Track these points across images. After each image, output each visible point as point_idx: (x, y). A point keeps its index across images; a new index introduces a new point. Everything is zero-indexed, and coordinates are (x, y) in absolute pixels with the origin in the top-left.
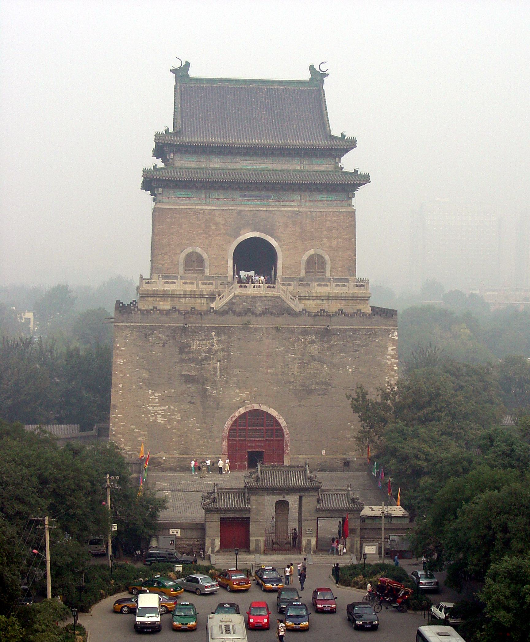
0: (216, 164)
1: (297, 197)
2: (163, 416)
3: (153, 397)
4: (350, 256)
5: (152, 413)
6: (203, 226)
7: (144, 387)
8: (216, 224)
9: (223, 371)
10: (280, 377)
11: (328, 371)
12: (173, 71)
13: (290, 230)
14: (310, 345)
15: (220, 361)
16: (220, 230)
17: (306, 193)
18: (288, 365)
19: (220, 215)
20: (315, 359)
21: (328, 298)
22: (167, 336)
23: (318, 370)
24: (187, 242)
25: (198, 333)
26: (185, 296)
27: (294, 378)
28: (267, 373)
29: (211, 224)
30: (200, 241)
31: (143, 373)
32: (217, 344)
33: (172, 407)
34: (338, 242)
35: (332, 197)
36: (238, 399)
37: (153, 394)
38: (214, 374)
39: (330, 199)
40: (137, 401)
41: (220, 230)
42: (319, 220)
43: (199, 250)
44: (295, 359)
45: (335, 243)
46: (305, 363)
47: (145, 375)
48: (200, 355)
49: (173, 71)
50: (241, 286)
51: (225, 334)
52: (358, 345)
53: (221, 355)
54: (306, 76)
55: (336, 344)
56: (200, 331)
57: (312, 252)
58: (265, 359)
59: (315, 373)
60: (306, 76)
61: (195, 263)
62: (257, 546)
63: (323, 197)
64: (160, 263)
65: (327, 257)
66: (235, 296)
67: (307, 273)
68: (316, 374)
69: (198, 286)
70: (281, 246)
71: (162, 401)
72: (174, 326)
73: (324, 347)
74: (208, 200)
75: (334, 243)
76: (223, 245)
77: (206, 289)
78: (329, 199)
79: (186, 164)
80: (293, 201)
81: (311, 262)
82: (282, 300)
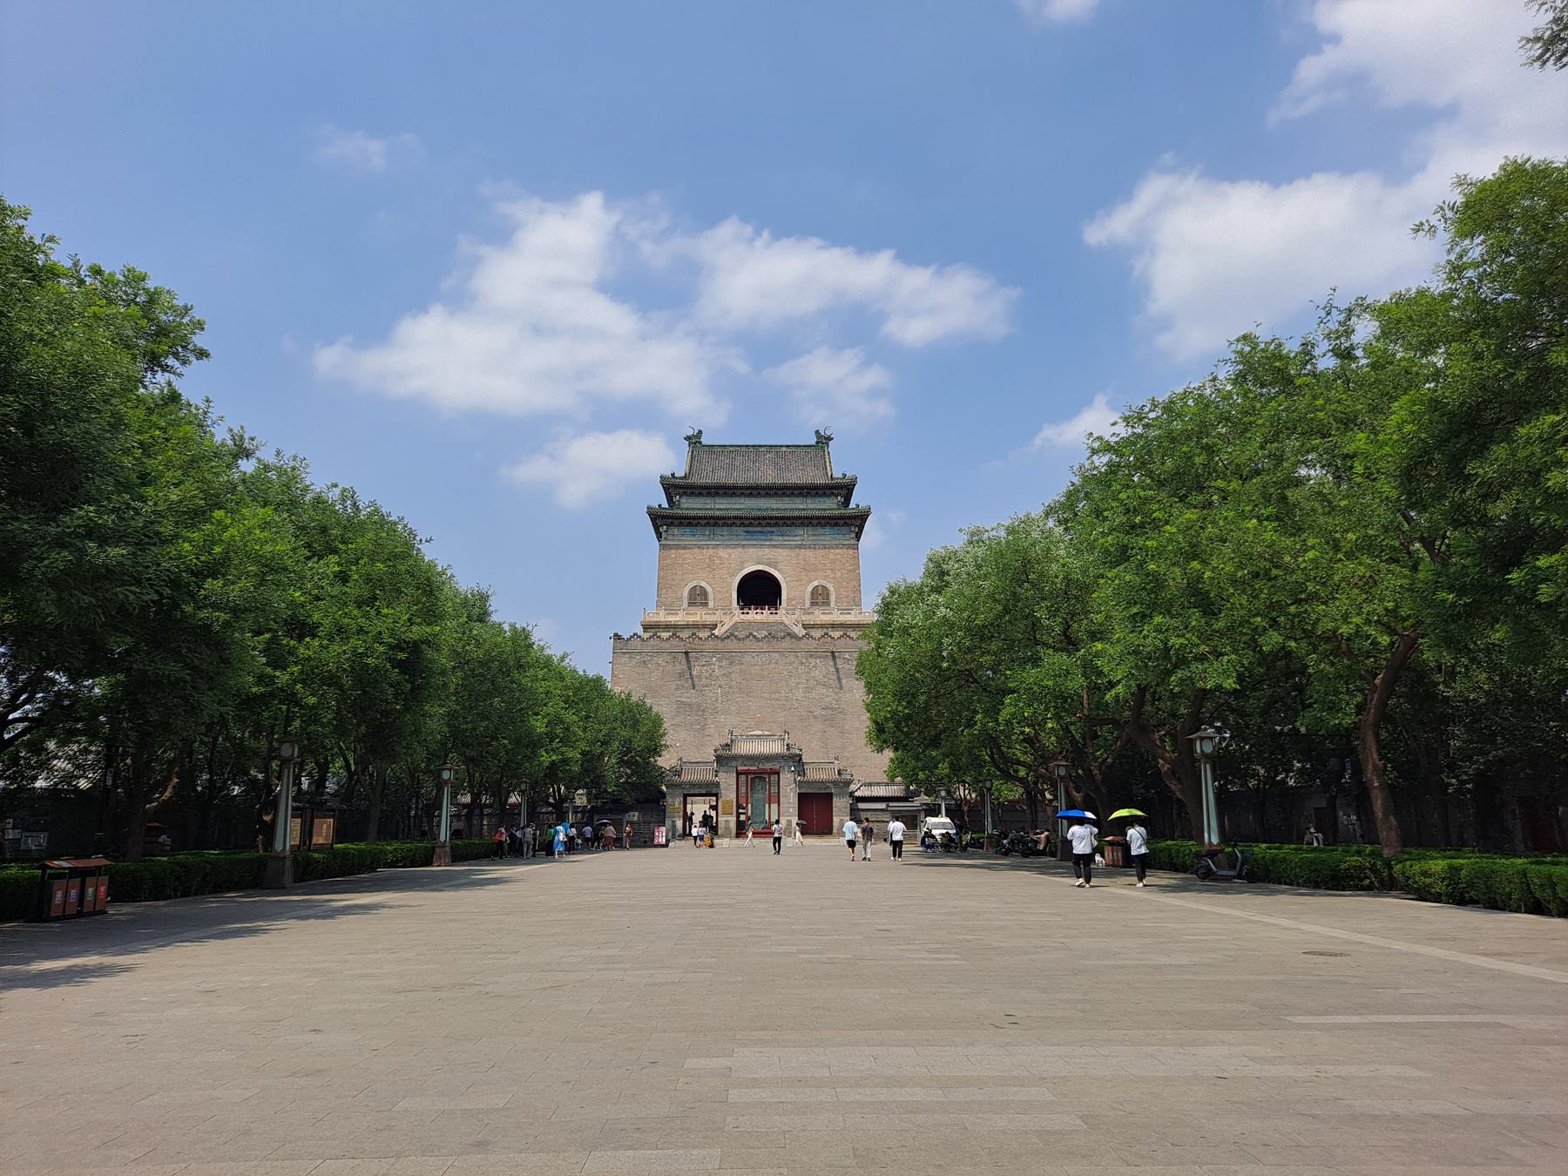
0: (720, 506)
8: (720, 558)
12: (688, 438)
21: (833, 626)
26: (687, 626)
43: (703, 584)
49: (688, 438)
54: (813, 441)
57: (816, 583)
60: (813, 441)
61: (698, 597)
62: (727, 828)
63: (827, 530)
65: (832, 589)
67: (813, 604)
77: (709, 619)
79: (691, 505)
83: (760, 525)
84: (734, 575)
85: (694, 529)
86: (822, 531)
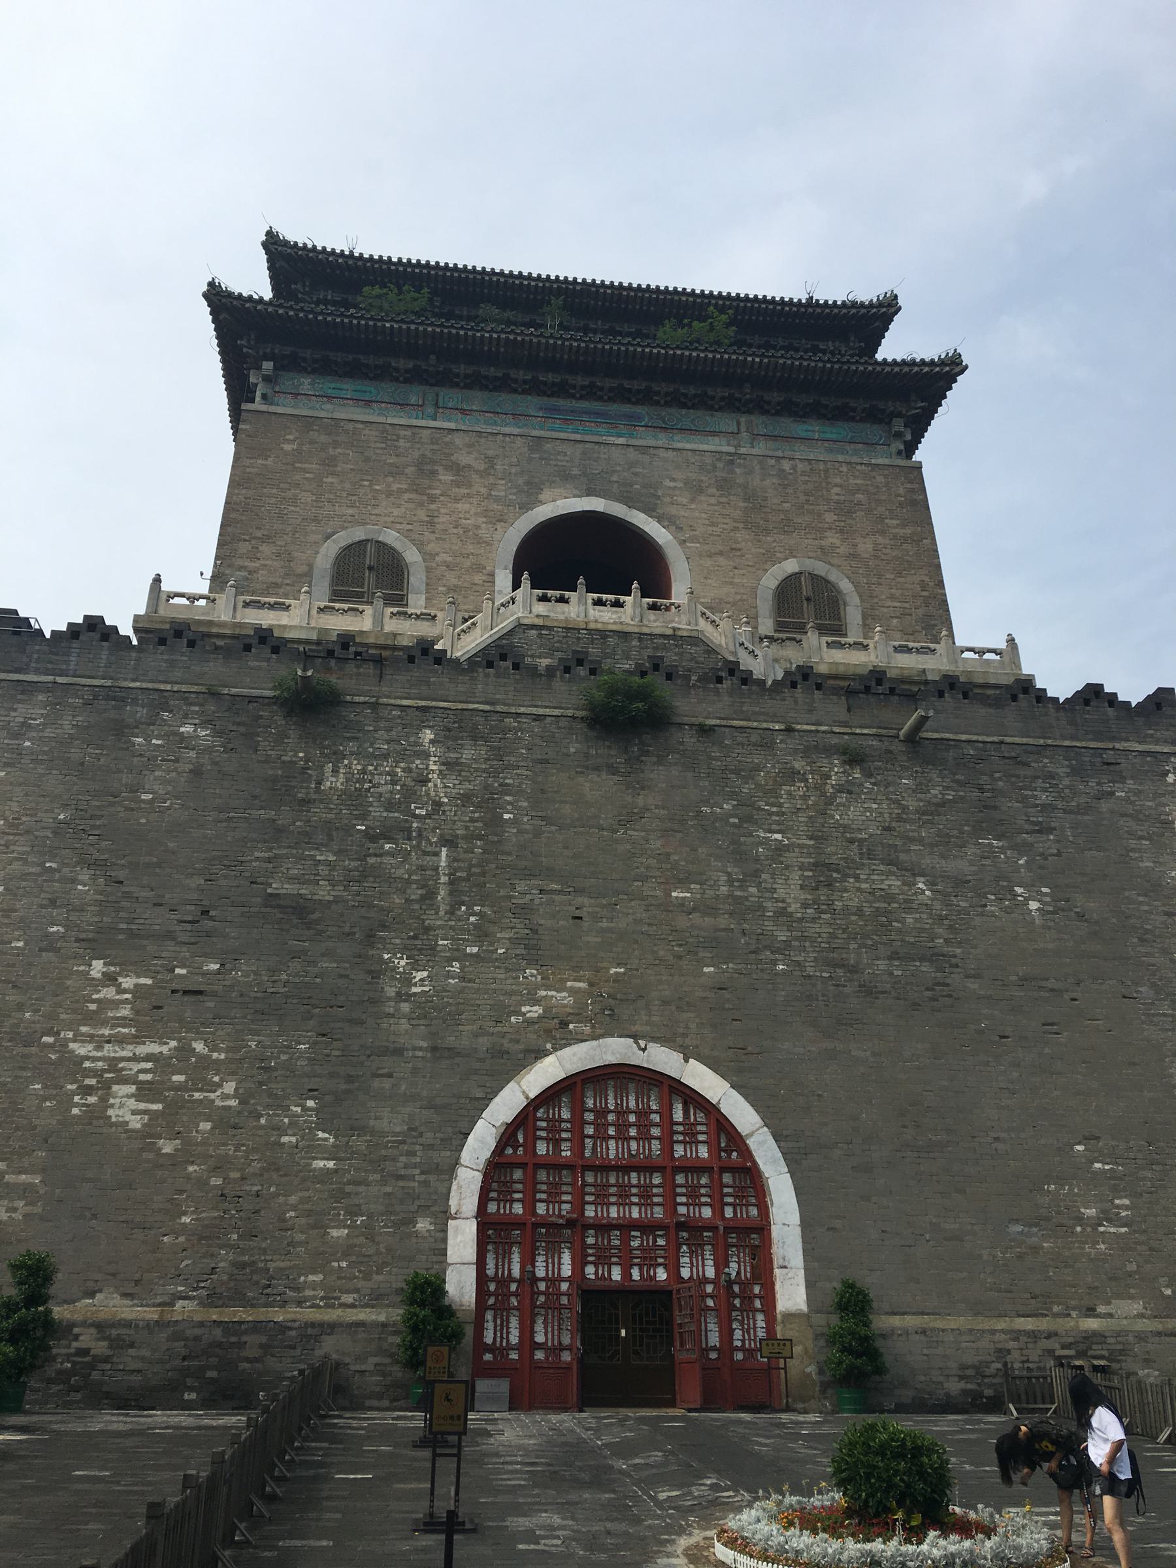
1: (726, 422)
2: (145, 1092)
3: (109, 993)
4: (924, 586)
5: (89, 1073)
6: (410, 470)
7: (74, 947)
8: (457, 469)
9: (464, 886)
10: (723, 921)
11: (937, 905)
13: (713, 501)
14: (842, 799)
15: (449, 842)
16: (470, 486)
17: (752, 417)
18: (756, 874)
19: (470, 446)
20: (870, 855)
22: (218, 733)
23: (889, 898)
24: (350, 511)
28: (667, 906)
29: (440, 469)
30: (396, 512)
31: (74, 881)
33: (199, 1046)
34: (876, 544)
35: (840, 430)
36: (535, 1011)
37: (110, 979)
38: (423, 898)
39: (833, 436)
40: (20, 1007)
41: (470, 486)
42: (806, 482)
43: (391, 537)
44: (787, 848)
45: (870, 547)
46: (829, 867)
47: (85, 886)
48: (363, 818)
50: (544, 599)
51: (476, 737)
52: (1045, 808)
53: (460, 821)
55: (954, 801)
57: (791, 566)
58: (656, 844)
64: (241, 568)
65: (845, 586)
66: (520, 627)
67: (780, 626)
68: (886, 913)
69: (378, 620)
70: (683, 543)
71: (151, 1015)
72: (252, 699)
73: (905, 808)
74: (430, 410)
75: (865, 547)
76: (478, 527)
78: (828, 436)
80: (714, 433)
81: (787, 592)
82: (710, 651)
83: (591, 393)
84: (502, 519)
85: (371, 389)
86: (800, 429)
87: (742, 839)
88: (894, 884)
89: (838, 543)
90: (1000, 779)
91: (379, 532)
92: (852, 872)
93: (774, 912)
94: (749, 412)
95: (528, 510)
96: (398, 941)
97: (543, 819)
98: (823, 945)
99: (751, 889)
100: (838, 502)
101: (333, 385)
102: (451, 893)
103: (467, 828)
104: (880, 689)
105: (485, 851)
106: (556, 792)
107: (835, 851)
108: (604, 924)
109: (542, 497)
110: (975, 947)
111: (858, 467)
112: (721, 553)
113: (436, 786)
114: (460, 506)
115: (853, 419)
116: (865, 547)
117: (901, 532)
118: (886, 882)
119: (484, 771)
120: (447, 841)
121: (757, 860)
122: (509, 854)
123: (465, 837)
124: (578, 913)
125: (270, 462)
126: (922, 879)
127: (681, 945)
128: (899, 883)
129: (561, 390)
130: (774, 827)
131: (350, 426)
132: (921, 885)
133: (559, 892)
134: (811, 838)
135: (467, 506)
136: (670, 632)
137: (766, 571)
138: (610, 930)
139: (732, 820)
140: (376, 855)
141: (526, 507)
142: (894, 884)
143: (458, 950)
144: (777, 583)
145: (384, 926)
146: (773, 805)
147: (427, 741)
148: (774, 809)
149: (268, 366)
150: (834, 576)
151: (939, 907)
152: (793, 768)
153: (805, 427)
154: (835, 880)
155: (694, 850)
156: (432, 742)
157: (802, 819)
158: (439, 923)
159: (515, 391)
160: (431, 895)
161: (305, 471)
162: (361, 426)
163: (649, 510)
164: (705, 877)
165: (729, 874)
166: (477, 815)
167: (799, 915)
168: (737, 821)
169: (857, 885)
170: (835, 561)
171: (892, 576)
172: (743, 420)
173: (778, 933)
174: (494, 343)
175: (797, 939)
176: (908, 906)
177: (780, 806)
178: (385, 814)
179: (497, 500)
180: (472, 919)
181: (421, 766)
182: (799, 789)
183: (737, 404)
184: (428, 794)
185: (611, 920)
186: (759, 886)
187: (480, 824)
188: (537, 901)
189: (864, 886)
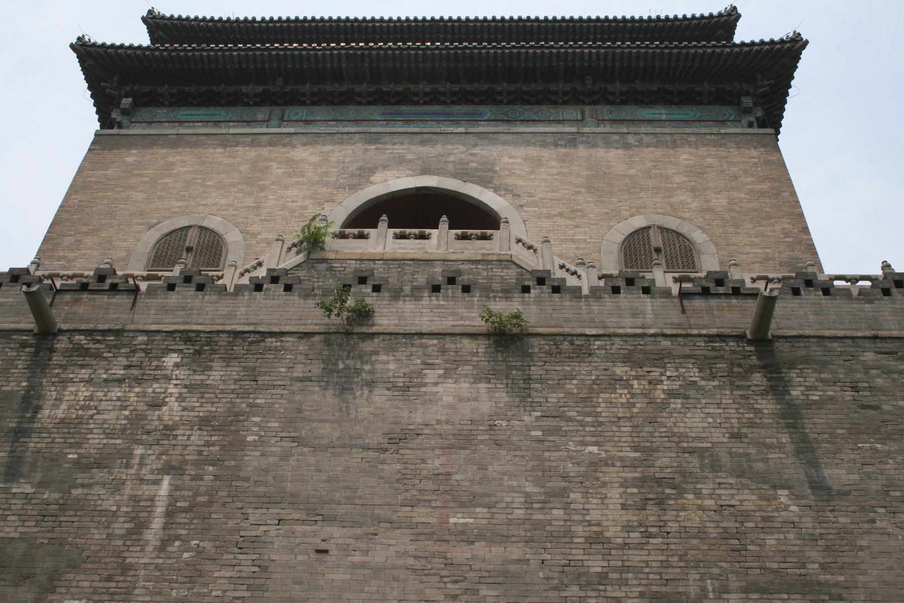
9: (181, 518)
10: (515, 551)
11: (808, 522)
14: (677, 404)
17: (598, 107)
18: (563, 493)
20: (716, 467)
23: (746, 515)
25: (98, 356)
27: (606, 556)
28: (444, 535)
32: (181, 398)
34: (731, 201)
38: (130, 532)
43: (214, 223)
45: (724, 202)
46: (659, 481)
55: (820, 404)
56: (110, 348)
57: (639, 222)
59: (726, 535)
65: (698, 237)
68: (739, 535)
73: (758, 411)
75: (720, 201)
80: (559, 122)
83: (434, 98)
85: (221, 113)
86: (646, 113)
87: (547, 454)
88: (749, 500)
89: (690, 200)
90: (879, 376)
91: (204, 218)
92: (691, 486)
93: (586, 538)
94: (594, 103)
95: (357, 190)
96: (86, 584)
97: (294, 439)
98: (651, 576)
99: (555, 512)
100: (687, 166)
101: (185, 113)
102: (165, 527)
103: (200, 453)
104: (721, 290)
105: (216, 477)
106: (316, 411)
107: (665, 461)
108: (357, 558)
109: (372, 179)
110: (864, 573)
111: (708, 137)
112: (560, 215)
113: (171, 410)
114: (289, 192)
115: (701, 103)
116: (720, 201)
117: (758, 187)
118: (737, 497)
119: (233, 391)
120: (172, 468)
121: (565, 478)
122: (247, 479)
123: (195, 463)
124: (323, 546)
125: (110, 172)
126: (786, 492)
127: (456, 582)
128: (754, 497)
129: (403, 99)
130: (588, 439)
131: (194, 138)
132: (783, 499)
133: (303, 522)
134: (636, 449)
135: (296, 192)
136: (479, 257)
137: (610, 228)
138: (363, 566)
139: (533, 433)
140: (83, 486)
141: (354, 188)
142: (749, 500)
143: (160, 593)
144: (622, 238)
145: (74, 566)
146: (588, 414)
147: (171, 364)
148: (589, 419)
149: (126, 102)
150: (685, 229)
151: (810, 525)
152: (614, 374)
153: (652, 111)
154: (669, 497)
155: (483, 467)
156: (177, 365)
157: (623, 429)
158: (143, 561)
159: (360, 104)
160: (140, 526)
161: (142, 176)
162: (203, 138)
163: (485, 182)
164: (494, 499)
165: (527, 495)
166: (214, 438)
167: (620, 541)
168: (540, 433)
169: (699, 502)
170: (687, 215)
171: (749, 226)
172: (588, 109)
173: (590, 563)
174: (336, 60)
175: (615, 569)
176: (767, 524)
177: (597, 415)
178: (105, 441)
179: (327, 184)
180: (186, 555)
181: (159, 390)
182: (622, 396)
183: (581, 97)
184: (160, 419)
185: (366, 552)
186: (566, 507)
187: (217, 448)
188: (273, 533)
189: (709, 503)
